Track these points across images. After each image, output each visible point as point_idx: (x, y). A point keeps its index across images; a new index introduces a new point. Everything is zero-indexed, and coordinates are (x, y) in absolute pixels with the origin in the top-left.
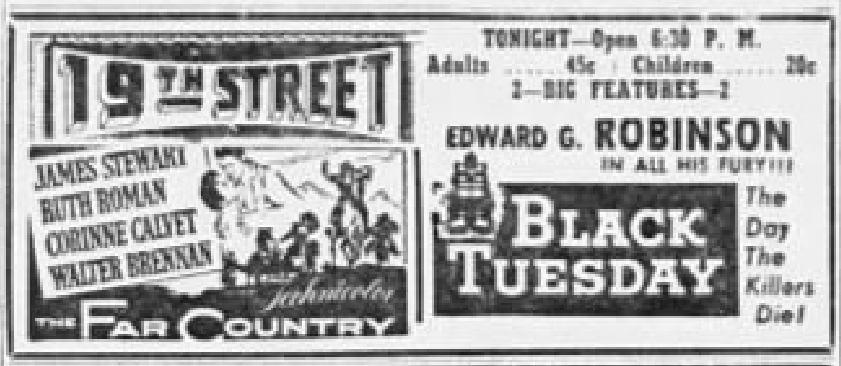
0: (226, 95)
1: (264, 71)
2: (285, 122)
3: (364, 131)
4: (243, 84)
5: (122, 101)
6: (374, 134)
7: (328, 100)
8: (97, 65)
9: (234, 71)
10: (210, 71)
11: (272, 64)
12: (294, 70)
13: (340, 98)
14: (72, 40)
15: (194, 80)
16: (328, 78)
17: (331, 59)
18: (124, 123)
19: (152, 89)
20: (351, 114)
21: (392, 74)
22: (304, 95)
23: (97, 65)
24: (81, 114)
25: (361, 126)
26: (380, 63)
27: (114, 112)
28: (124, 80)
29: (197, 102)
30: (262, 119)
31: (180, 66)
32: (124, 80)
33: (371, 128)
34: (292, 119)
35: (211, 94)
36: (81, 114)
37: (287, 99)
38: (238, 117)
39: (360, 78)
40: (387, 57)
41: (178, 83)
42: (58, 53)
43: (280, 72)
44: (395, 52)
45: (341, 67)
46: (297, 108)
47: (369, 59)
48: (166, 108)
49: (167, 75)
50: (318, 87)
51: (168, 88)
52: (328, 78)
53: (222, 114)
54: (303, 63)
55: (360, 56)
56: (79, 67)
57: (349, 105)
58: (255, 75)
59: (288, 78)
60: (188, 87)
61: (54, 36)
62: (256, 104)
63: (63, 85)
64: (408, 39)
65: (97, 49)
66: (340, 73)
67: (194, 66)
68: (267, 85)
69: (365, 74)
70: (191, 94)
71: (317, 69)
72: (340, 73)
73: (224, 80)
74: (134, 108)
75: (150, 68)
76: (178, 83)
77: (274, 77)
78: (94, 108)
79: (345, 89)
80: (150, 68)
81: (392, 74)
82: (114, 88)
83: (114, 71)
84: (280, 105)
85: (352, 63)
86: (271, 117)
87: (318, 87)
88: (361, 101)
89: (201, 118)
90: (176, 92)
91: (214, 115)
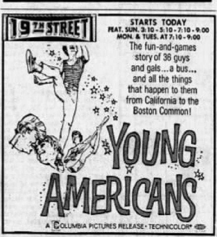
0: (49, 29)
1: (58, 23)
2: (63, 35)
3: (82, 39)
4: (53, 27)
5: (24, 30)
6: (84, 39)
7: (73, 31)
8: (19, 21)
9: (51, 23)
10: (45, 23)
11: (60, 22)
12: (65, 23)
13: (76, 30)
14: (14, 15)
15: (42, 25)
16: (73, 25)
17: (73, 20)
18: (24, 36)
19: (32, 27)
20: (78, 34)
21: (88, 24)
22: (67, 29)
23: (19, 21)
24: (15, 33)
25: (81, 37)
26: (85, 22)
27: (23, 33)
28: (25, 25)
29: (42, 31)
30: (58, 35)
31: (39, 22)
32: (25, 25)
33: (83, 38)
34: (65, 35)
35: (46, 29)
36: (15, 33)
37: (63, 30)
38: (53, 35)
39: (80, 25)
40: (86, 21)
41: (38, 26)
42: (9, 19)
43: (62, 23)
44: (89, 19)
45: (76, 22)
46: (66, 32)
47: (83, 21)
48: (35, 33)
49: (35, 24)
50: (70, 28)
51: (36, 27)
52: (73, 25)
53: (49, 34)
54: (67, 21)
55: (80, 20)
56: (14, 22)
57: (78, 32)
58: (56, 25)
59: (64, 25)
60: (40, 27)
61: (8, 14)
62: (56, 31)
63: (10, 27)
64: (92, 15)
65: (19, 18)
66: (76, 25)
67: (42, 22)
68: (59, 28)
69: (81, 24)
70: (41, 29)
71: (70, 23)
72: (76, 25)
73: (49, 25)
74: (28, 32)
75: (31, 22)
76: (38, 26)
77: (60, 24)
78: (18, 32)
79: (77, 28)
80: (31, 22)
81: (88, 24)
82: (22, 27)
83: (22, 23)
84: (62, 32)
85: (78, 21)
86: (60, 35)
87: (70, 28)
88: (80, 31)
89: (44, 35)
90: (37, 28)
91: (46, 34)
